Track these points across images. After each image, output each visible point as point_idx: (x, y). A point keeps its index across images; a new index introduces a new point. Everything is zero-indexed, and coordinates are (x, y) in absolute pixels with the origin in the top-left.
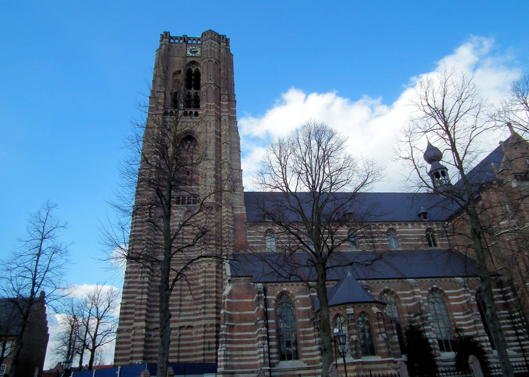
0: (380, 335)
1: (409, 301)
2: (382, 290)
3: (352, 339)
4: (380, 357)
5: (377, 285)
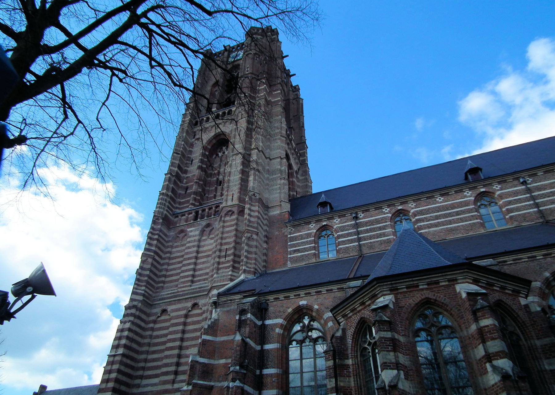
0: (488, 365)
3: (383, 382)
5: (531, 264)
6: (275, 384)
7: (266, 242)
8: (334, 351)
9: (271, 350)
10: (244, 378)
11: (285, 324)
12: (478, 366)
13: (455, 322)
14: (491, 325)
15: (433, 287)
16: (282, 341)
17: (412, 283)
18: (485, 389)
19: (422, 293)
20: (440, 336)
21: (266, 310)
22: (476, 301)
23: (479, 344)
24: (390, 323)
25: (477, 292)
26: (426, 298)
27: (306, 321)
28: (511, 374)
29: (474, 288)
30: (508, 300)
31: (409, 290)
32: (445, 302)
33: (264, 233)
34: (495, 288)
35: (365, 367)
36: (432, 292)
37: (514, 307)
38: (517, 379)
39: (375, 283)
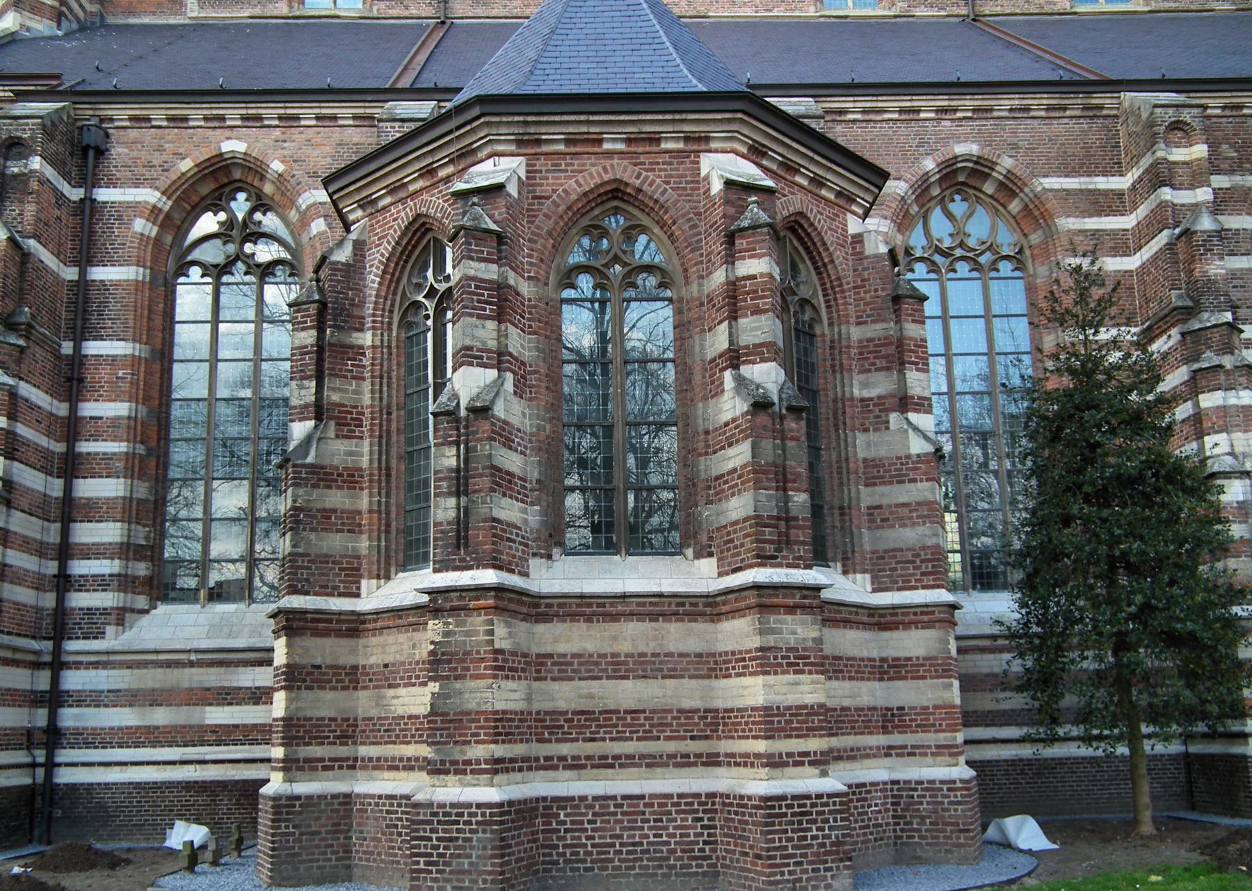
0: (728, 375)
1: (1122, 244)
2: (929, 164)
3: (455, 396)
4: (708, 566)
5: (903, 130)
6: (125, 386)
8: (323, 305)
9: (116, 284)
10: (19, 362)
11: (167, 208)
12: (704, 377)
13: (676, 261)
14: (762, 275)
15: (640, 150)
16: (155, 259)
17: (584, 129)
18: (707, 432)
19: (608, 163)
20: (631, 293)
21: (101, 152)
22: (742, 209)
23: (720, 322)
24: (500, 238)
25: (751, 181)
26: (615, 180)
27: (241, 205)
28: (776, 399)
29: (747, 171)
30: (819, 218)
31: (572, 149)
32: (662, 200)
34: (798, 179)
35: (409, 357)
36: (635, 165)
37: (829, 238)
38: (784, 411)
39: (476, 111)
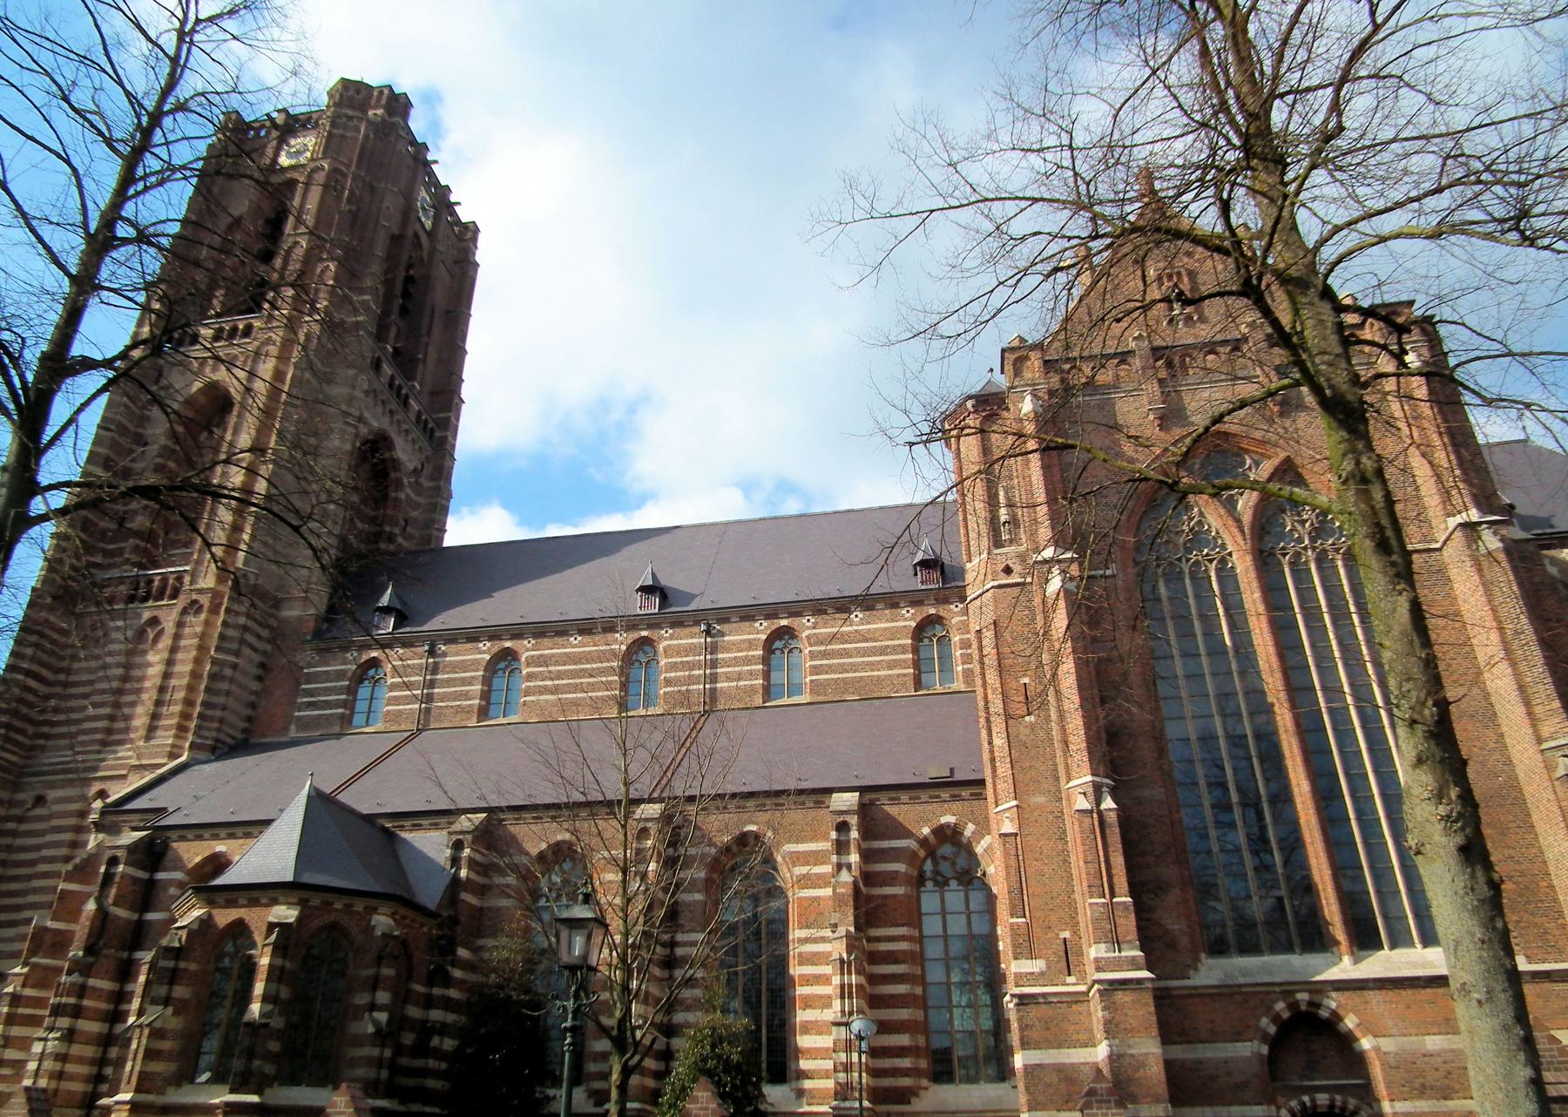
7: (259, 678)
33: (257, 658)
